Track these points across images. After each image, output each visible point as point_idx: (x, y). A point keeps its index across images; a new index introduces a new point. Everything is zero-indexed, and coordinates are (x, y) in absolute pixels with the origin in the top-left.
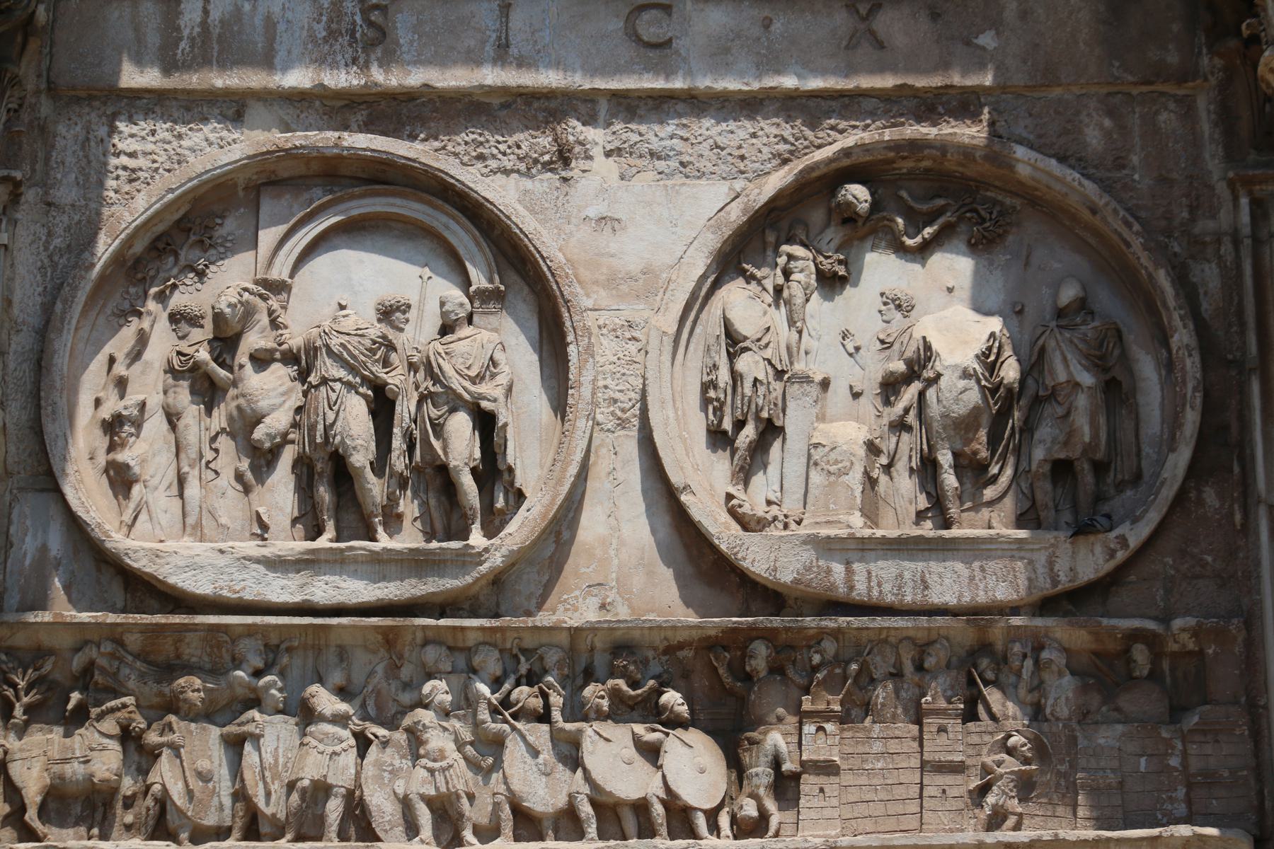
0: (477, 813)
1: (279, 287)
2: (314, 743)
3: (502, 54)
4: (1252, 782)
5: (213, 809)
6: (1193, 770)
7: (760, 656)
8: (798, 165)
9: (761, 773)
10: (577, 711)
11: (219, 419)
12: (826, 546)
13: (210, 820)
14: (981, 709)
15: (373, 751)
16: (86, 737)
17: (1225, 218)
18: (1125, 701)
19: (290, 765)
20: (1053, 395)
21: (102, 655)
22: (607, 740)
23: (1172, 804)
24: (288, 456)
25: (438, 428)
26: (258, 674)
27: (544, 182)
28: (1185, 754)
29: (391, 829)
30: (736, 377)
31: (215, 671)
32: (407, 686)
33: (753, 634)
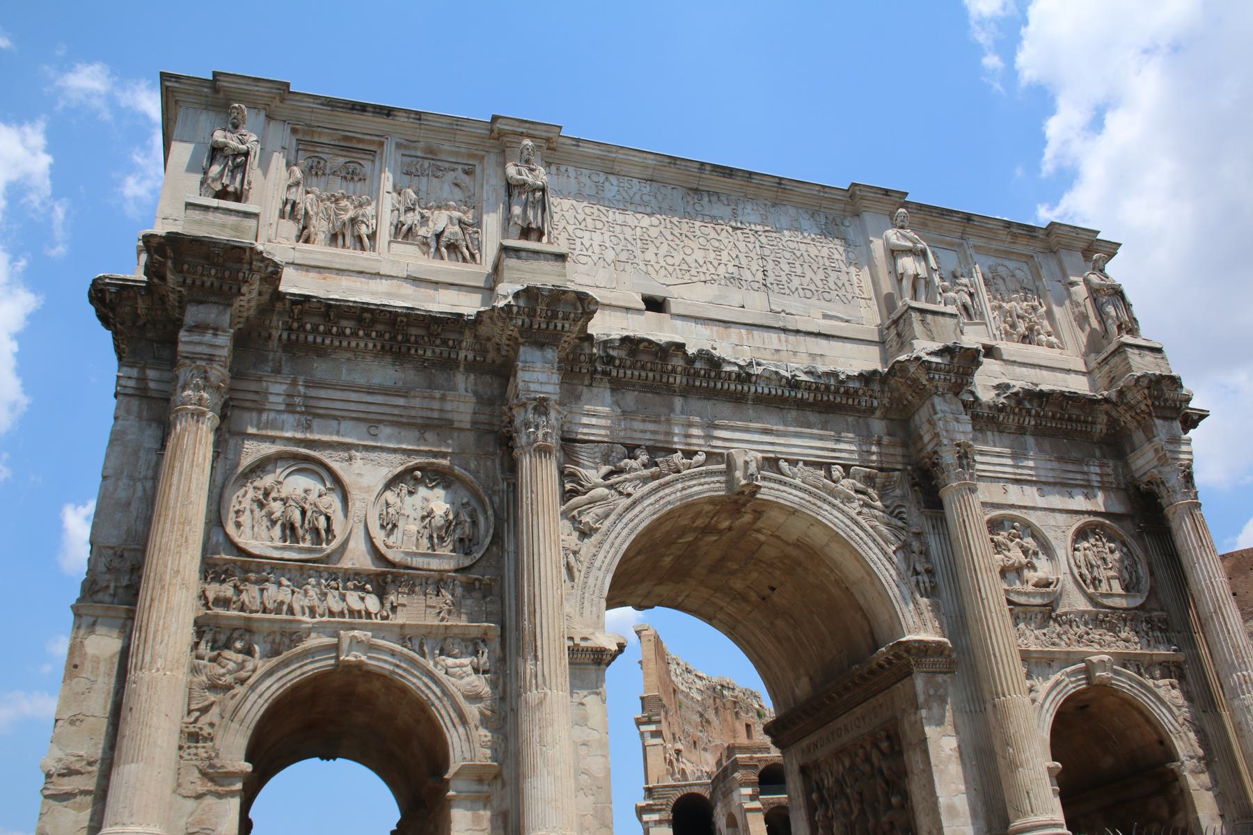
1: (280, 483)
3: (338, 433)
7: (390, 578)
8: (405, 466)
9: (388, 605)
10: (345, 588)
11: (263, 513)
12: (407, 554)
13: (254, 608)
16: (225, 586)
17: (501, 486)
20: (460, 523)
24: (279, 523)
25: (317, 519)
27: (345, 464)
30: (388, 513)
31: (258, 572)
33: (388, 573)
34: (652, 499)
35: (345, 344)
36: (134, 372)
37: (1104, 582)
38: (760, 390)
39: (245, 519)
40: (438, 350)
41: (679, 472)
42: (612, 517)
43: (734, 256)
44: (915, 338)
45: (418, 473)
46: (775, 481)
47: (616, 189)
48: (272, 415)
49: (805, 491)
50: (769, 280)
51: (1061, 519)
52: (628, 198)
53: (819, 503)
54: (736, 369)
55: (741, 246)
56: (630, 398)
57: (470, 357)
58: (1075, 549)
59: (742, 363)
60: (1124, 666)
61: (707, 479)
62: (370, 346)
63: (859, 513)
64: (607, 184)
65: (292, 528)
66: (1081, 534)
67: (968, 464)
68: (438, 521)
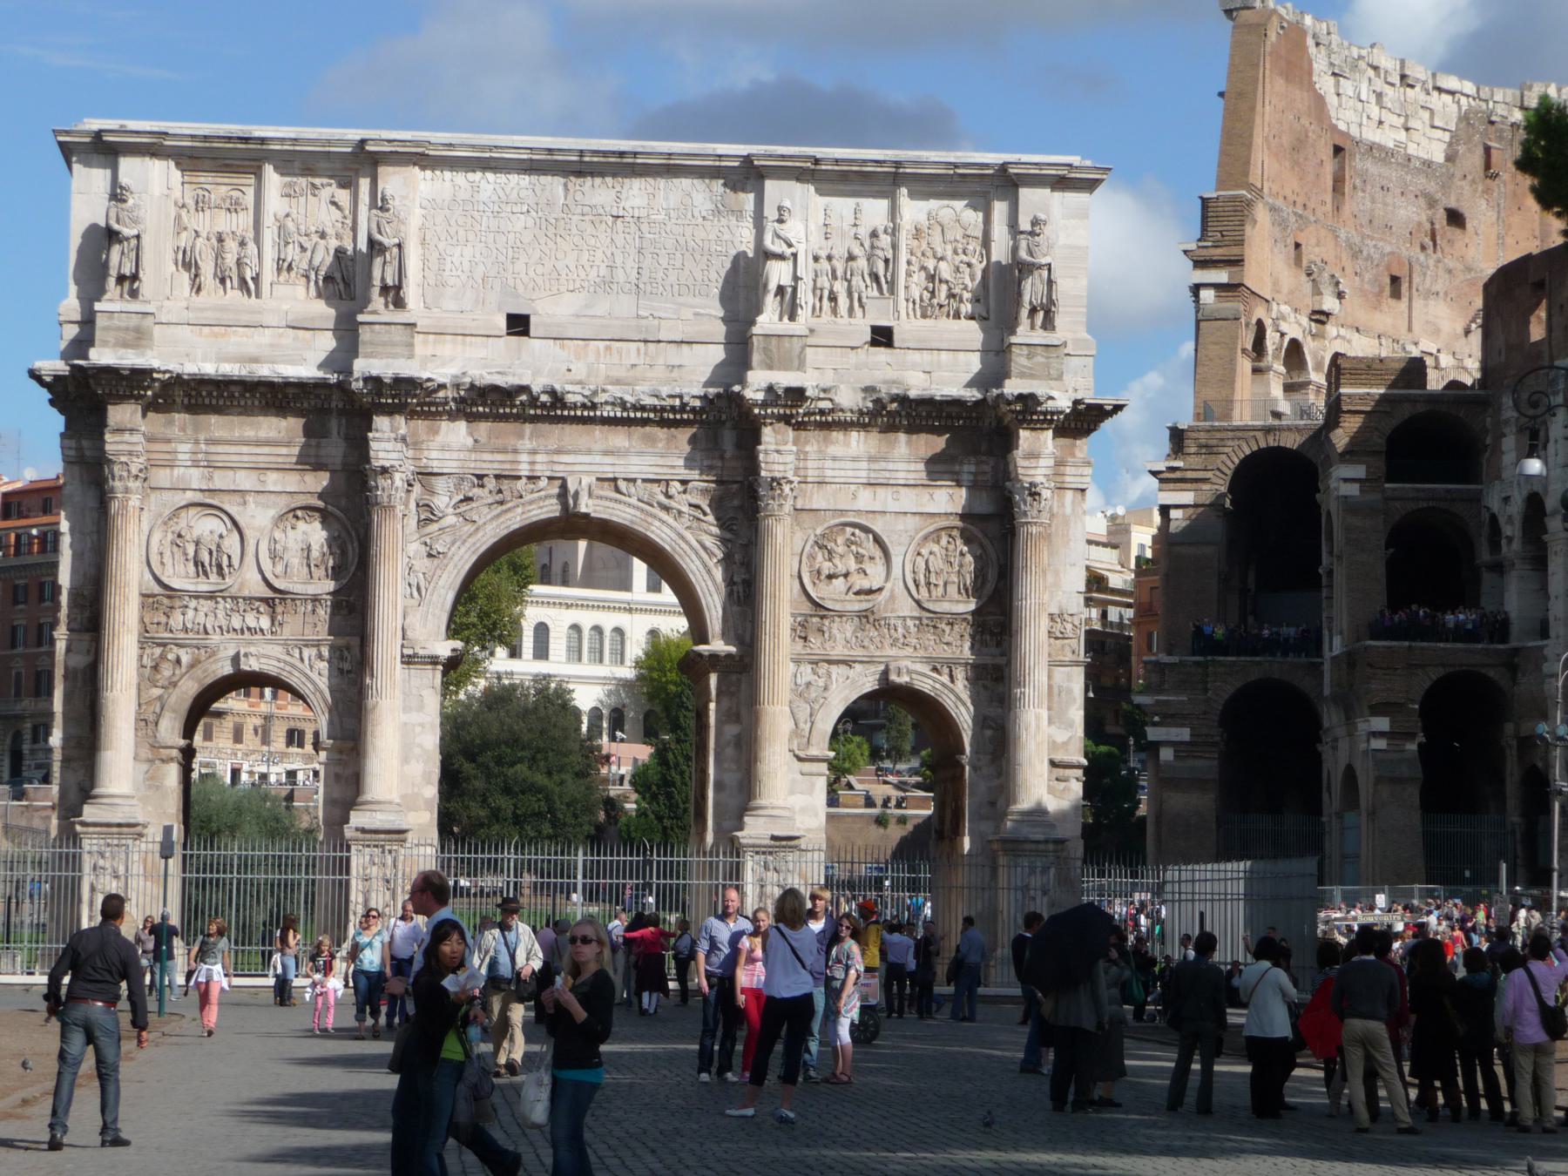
0: (225, 628)
7: (277, 601)
27: (241, 508)
34: (495, 524)
35: (235, 403)
36: (73, 443)
37: (941, 583)
38: (605, 414)
39: (167, 559)
40: (313, 403)
41: (521, 497)
42: (458, 544)
43: (609, 255)
44: (750, 368)
45: (299, 513)
46: (611, 500)
47: (491, 187)
48: (182, 470)
49: (638, 508)
50: (645, 278)
51: (910, 520)
52: (504, 198)
53: (650, 520)
54: (579, 399)
55: (619, 241)
56: (483, 427)
57: (340, 406)
58: (919, 554)
59: (587, 393)
60: (935, 669)
61: (547, 502)
62: (257, 403)
63: (688, 528)
64: (483, 184)
65: (203, 565)
66: (934, 536)
67: (780, 495)
68: (315, 554)
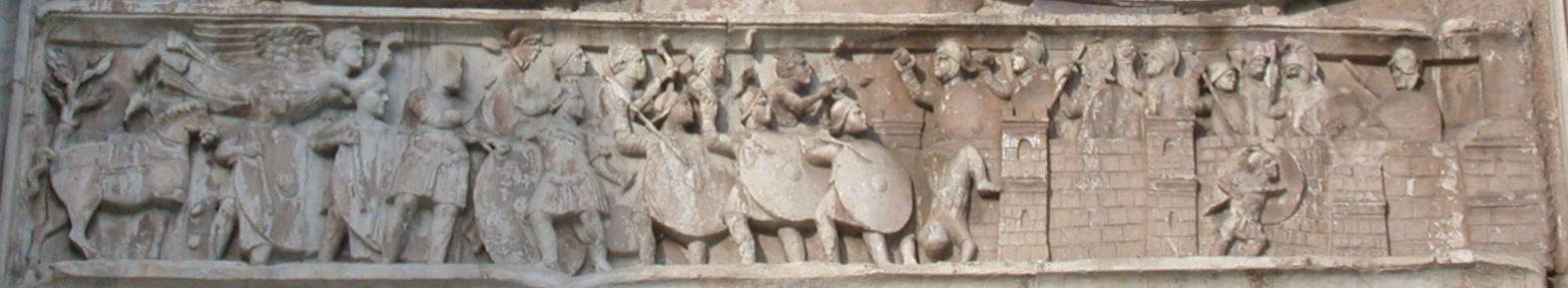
2: (420, 153)
4: (1543, 206)
5: (296, 231)
6: (1471, 192)
13: (292, 243)
14: (1216, 122)
15: (490, 159)
18: (1387, 116)
19: (390, 179)
21: (170, 50)
22: (769, 153)
23: (1446, 233)
26: (354, 73)
28: (1461, 175)
29: (510, 253)
32: (529, 93)
